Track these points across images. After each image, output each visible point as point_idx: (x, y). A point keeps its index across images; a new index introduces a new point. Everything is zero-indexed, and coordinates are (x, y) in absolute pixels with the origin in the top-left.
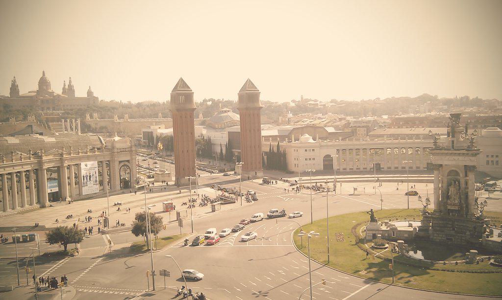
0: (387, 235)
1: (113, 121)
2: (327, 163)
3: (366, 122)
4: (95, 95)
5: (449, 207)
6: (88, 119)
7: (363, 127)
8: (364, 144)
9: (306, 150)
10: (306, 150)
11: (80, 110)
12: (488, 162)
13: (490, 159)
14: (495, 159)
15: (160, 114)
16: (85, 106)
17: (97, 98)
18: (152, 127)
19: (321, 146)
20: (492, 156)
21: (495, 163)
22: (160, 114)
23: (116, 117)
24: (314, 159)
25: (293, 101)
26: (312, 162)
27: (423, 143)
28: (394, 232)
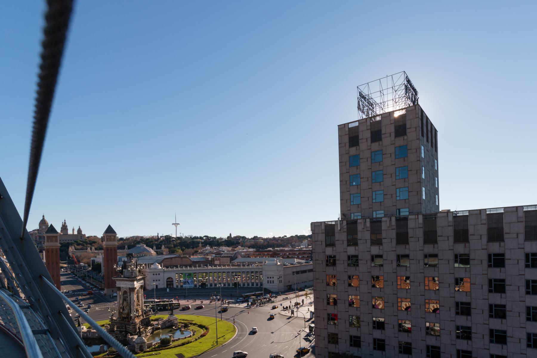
0: (85, 335)
1: (87, 251)
2: (169, 283)
3: (231, 254)
4: (83, 233)
5: (123, 316)
6: (70, 250)
7: (229, 257)
8: (195, 270)
9: (154, 274)
10: (154, 274)
11: (68, 243)
12: (268, 281)
13: (269, 279)
14: (272, 279)
15: (126, 247)
16: (74, 240)
17: (85, 235)
18: (98, 256)
19: (164, 271)
20: (271, 278)
21: (272, 282)
22: (126, 247)
23: (89, 249)
24: (159, 280)
25: (228, 237)
26: (157, 283)
27: (232, 269)
28: (89, 333)
